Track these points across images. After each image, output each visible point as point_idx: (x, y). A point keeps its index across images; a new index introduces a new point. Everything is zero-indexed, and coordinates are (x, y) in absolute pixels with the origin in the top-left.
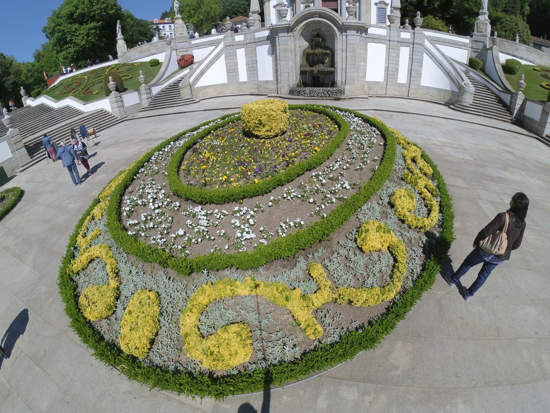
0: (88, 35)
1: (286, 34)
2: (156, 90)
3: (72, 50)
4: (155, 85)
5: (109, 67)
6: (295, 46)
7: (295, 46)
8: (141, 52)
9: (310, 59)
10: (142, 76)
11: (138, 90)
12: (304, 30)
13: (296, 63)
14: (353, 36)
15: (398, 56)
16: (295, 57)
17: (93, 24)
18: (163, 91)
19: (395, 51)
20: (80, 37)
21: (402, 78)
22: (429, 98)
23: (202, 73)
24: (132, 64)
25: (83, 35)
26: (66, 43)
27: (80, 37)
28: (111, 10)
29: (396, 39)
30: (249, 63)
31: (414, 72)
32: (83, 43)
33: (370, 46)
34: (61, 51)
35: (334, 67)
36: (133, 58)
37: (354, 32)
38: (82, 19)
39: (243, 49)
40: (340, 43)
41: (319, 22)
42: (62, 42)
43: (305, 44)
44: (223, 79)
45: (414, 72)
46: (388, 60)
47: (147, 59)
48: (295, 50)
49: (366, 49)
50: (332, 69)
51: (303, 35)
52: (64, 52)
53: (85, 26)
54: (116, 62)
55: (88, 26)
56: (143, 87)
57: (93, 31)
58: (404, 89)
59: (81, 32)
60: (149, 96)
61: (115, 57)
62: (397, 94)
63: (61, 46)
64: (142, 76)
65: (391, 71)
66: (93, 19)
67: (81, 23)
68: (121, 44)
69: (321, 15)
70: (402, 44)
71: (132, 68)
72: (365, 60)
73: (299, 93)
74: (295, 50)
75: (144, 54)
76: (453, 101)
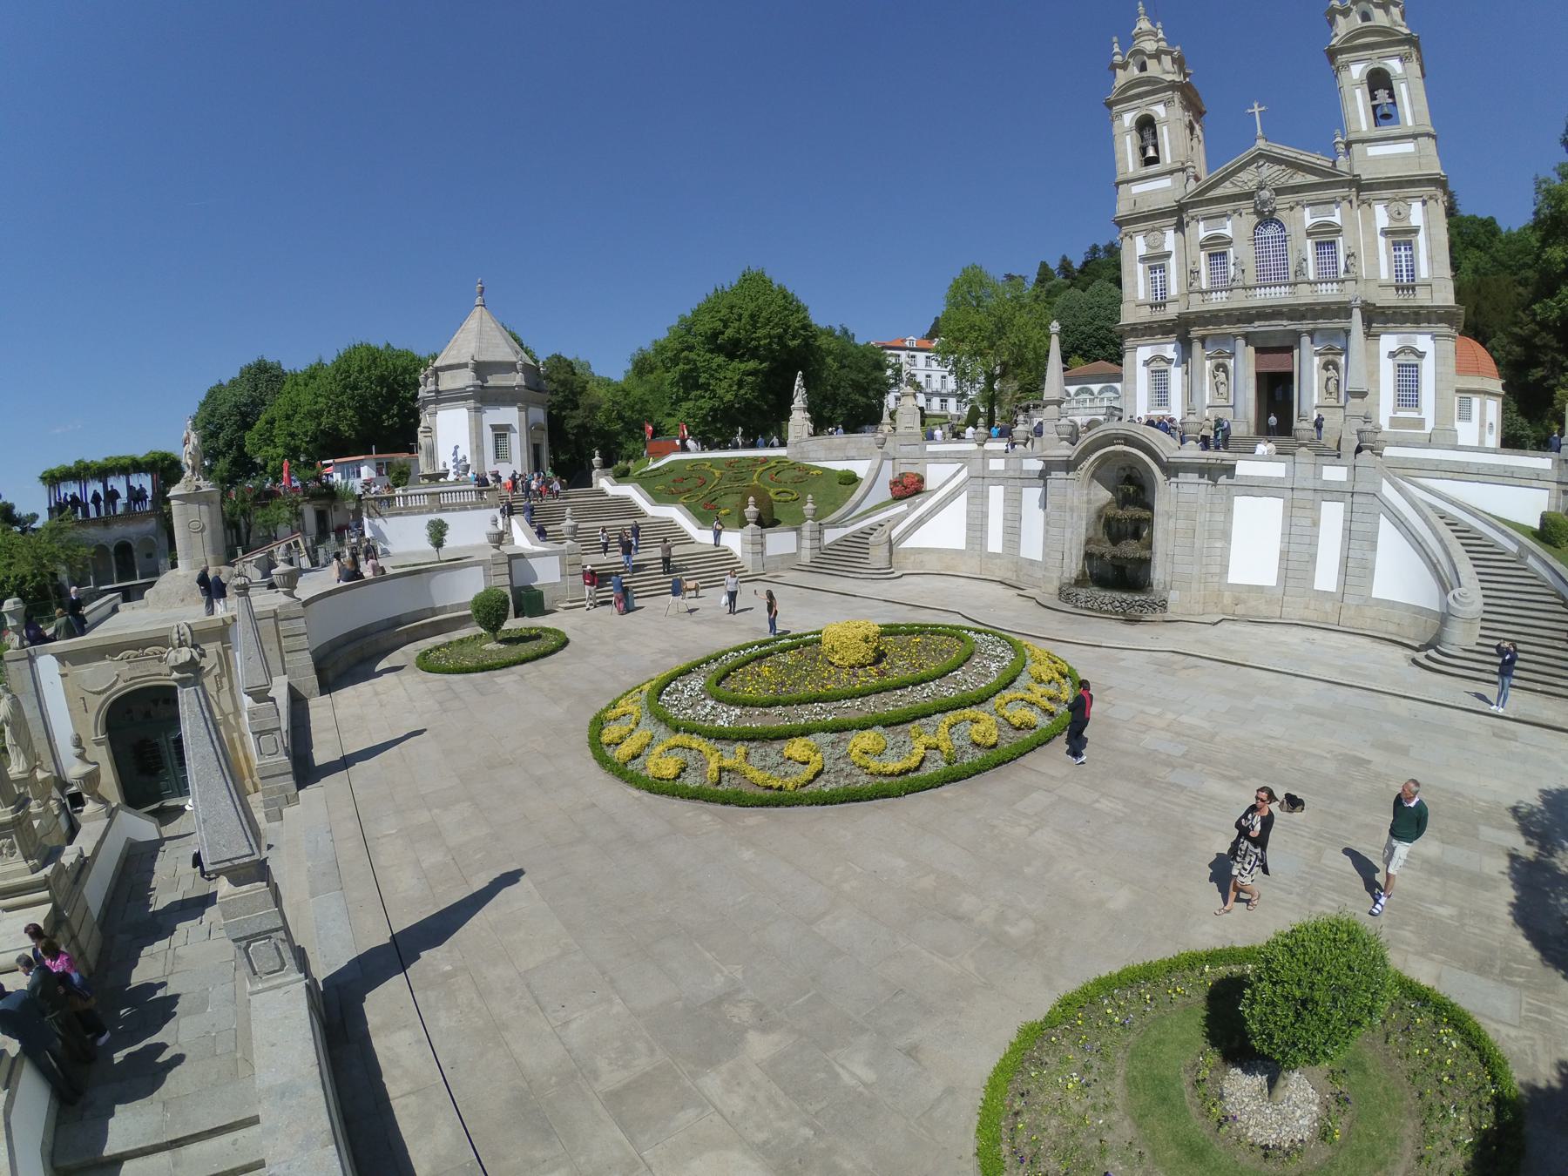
0: (740, 384)
1: (1062, 474)
2: (831, 536)
3: (706, 404)
4: (834, 525)
5: (766, 460)
8: (829, 449)
10: (810, 506)
11: (798, 530)
12: (1098, 467)
14: (1191, 487)
15: (1316, 523)
17: (752, 365)
18: (845, 539)
19: (1308, 513)
20: (724, 384)
21: (1326, 577)
22: (1390, 630)
24: (807, 469)
25: (731, 380)
26: (698, 387)
27: (724, 384)
28: (794, 338)
31: (1356, 566)
32: (729, 397)
33: (1242, 504)
34: (687, 399)
36: (812, 455)
37: (1193, 477)
38: (733, 350)
42: (690, 382)
43: (1104, 495)
45: (1356, 566)
46: (1288, 534)
47: (839, 466)
52: (690, 404)
53: (735, 364)
54: (782, 452)
55: (742, 366)
56: (808, 526)
57: (750, 379)
58: (1328, 606)
59: (729, 374)
60: (816, 543)
61: (783, 444)
62: (1311, 615)
63: (687, 391)
64: (810, 506)
65: (1296, 558)
66: (754, 354)
67: (731, 356)
68: (799, 421)
69: (1128, 440)
71: (804, 477)
72: (1226, 536)
75: (835, 454)
76: (1429, 648)
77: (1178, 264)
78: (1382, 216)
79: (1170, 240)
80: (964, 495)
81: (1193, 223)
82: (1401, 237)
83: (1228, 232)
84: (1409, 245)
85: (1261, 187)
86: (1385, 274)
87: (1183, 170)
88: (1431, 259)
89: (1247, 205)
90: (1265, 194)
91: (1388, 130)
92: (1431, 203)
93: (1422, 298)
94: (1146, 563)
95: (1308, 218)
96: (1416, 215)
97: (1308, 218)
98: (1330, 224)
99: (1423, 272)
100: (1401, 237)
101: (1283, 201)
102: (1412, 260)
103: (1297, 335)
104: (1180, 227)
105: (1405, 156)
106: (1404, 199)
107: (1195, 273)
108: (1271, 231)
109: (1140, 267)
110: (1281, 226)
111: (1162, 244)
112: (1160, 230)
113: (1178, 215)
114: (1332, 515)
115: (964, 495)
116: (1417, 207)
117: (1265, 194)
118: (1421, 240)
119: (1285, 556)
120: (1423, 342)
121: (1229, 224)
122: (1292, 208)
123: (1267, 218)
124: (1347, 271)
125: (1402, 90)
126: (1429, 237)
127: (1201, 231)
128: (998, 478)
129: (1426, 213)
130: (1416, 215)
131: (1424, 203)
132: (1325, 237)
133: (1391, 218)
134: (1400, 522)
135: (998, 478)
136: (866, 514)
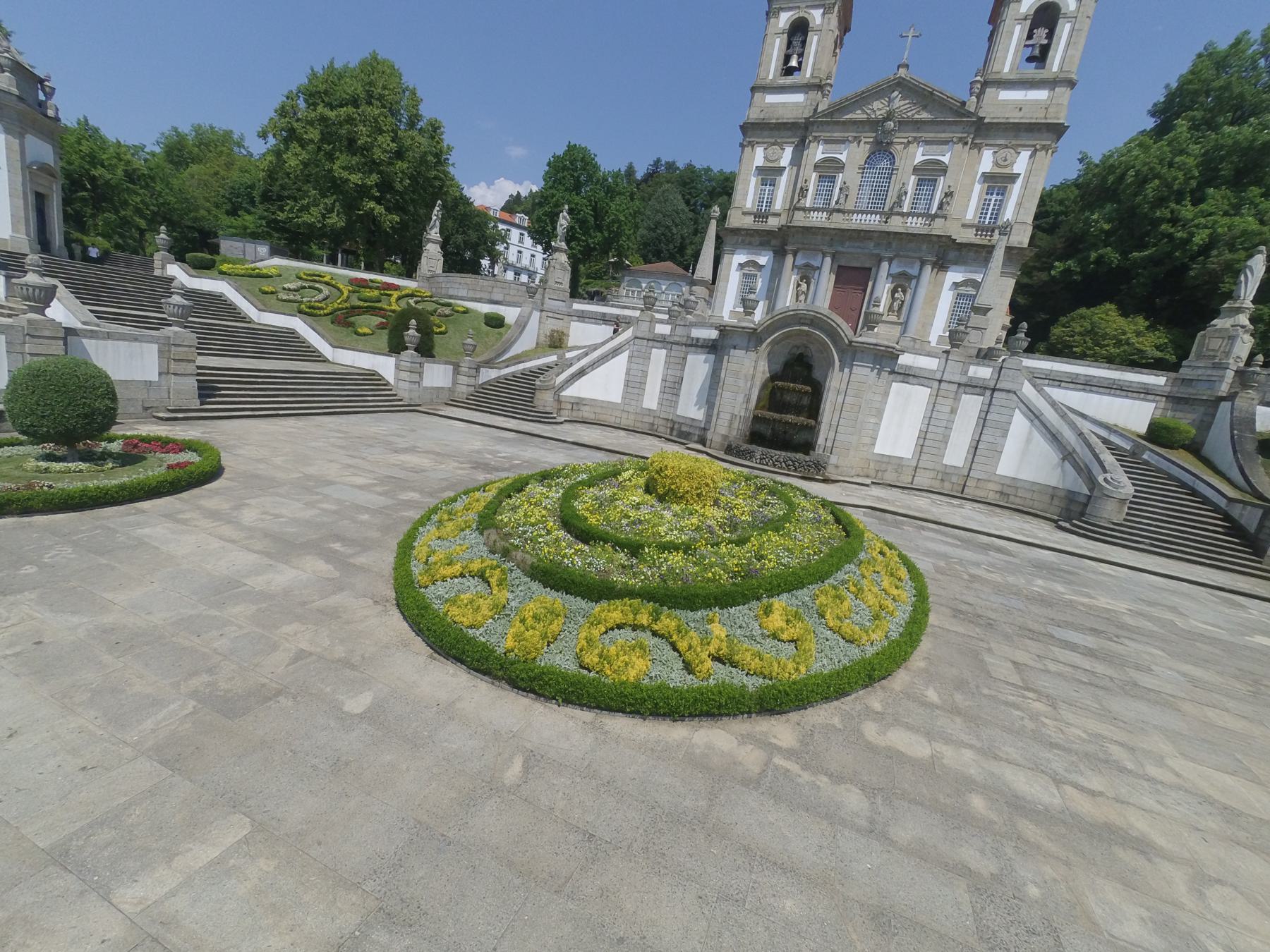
6: (749, 372)
7: (755, 368)
9: (773, 397)
13: (748, 402)
16: (751, 389)
19: (950, 402)
21: (956, 456)
23: (581, 373)
29: (957, 378)
30: (669, 378)
35: (816, 420)
39: (664, 352)
40: (835, 382)
41: (808, 334)
44: (615, 395)
48: (754, 376)
49: (886, 394)
50: (812, 422)
51: (771, 357)
70: (968, 389)
73: (740, 454)
74: (754, 376)
77: (789, 181)
80: (626, 354)
82: (998, 182)
84: (1003, 192)
88: (1019, 205)
94: (813, 430)
98: (939, 162)
99: (1008, 214)
102: (1000, 205)
111: (778, 160)
114: (971, 405)
115: (626, 354)
119: (923, 436)
128: (662, 341)
134: (1034, 416)
135: (662, 341)
136: (518, 359)
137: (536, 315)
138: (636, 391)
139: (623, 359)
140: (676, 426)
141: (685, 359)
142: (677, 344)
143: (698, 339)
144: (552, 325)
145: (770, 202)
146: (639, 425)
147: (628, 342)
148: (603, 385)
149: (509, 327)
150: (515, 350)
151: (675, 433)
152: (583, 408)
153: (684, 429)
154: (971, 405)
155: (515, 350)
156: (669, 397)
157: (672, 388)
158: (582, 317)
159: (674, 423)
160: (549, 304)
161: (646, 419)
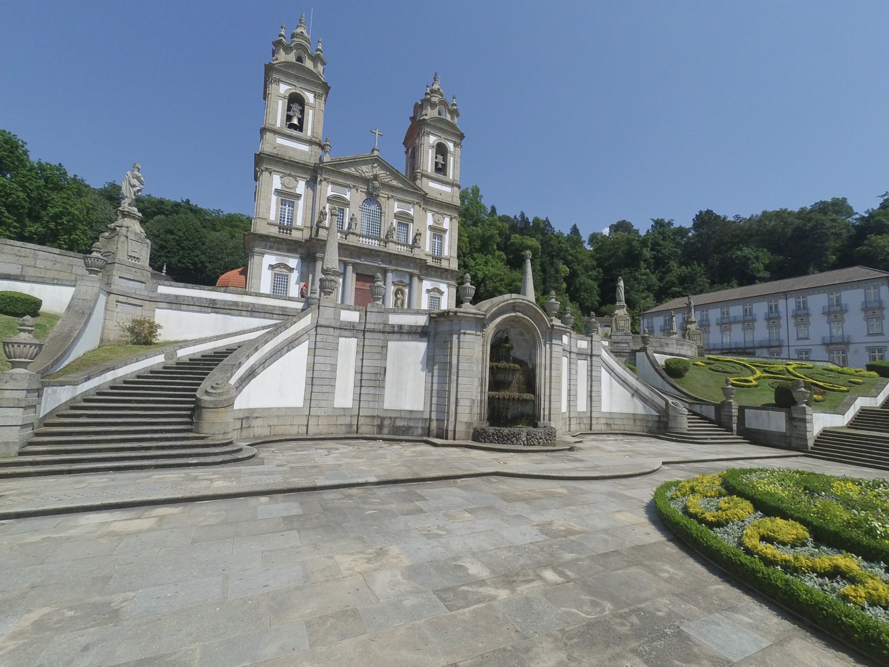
78: (430, 220)
79: (301, 187)
81: (324, 183)
82: (438, 233)
83: (348, 197)
84: (441, 238)
85: (376, 177)
86: (428, 249)
87: (322, 147)
88: (450, 247)
89: (363, 188)
90: (377, 184)
91: (440, 176)
92: (454, 220)
93: (444, 264)
95: (396, 207)
96: (446, 223)
97: (396, 207)
98: (408, 214)
99: (446, 253)
100: (438, 233)
101: (383, 193)
102: (441, 245)
103: (385, 272)
104: (312, 183)
105: (446, 193)
106: (442, 214)
107: (323, 214)
108: (373, 207)
109: (274, 198)
110: (380, 205)
112: (295, 177)
113: (314, 174)
116: (447, 220)
117: (377, 184)
118: (447, 236)
120: (443, 287)
121: (348, 194)
122: (388, 198)
123: (372, 197)
124: (415, 240)
125: (451, 160)
126: (451, 236)
127: (330, 190)
129: (451, 225)
130: (446, 223)
131: (451, 219)
132: (404, 220)
133: (435, 221)
136: (89, 366)
137: (103, 298)
138: (325, 389)
139: (302, 351)
140: (386, 422)
141: (385, 347)
142: (373, 331)
143: (401, 326)
144: (125, 315)
145: (292, 219)
146: (333, 429)
147: (306, 331)
148: (276, 388)
149: (53, 317)
150: (79, 351)
151: (386, 430)
152: (255, 423)
153: (400, 423)
154: (583, 365)
155: (79, 351)
156: (371, 391)
157: (372, 379)
158: (175, 303)
159: (383, 419)
160: (119, 284)
161: (342, 420)
